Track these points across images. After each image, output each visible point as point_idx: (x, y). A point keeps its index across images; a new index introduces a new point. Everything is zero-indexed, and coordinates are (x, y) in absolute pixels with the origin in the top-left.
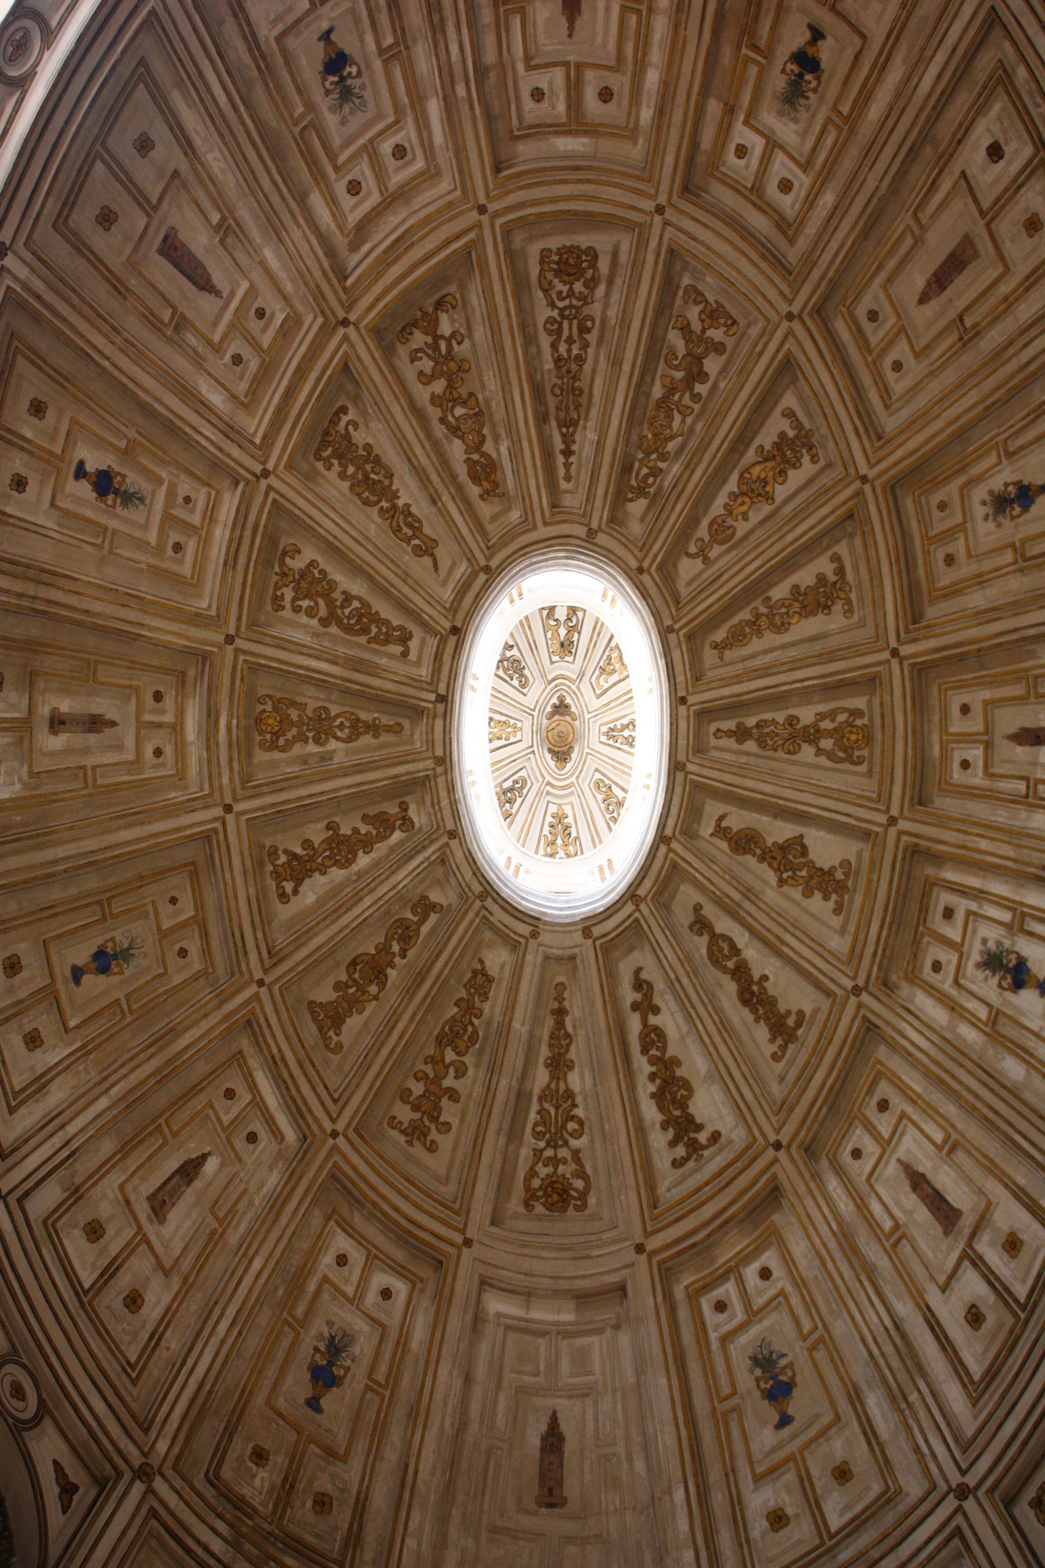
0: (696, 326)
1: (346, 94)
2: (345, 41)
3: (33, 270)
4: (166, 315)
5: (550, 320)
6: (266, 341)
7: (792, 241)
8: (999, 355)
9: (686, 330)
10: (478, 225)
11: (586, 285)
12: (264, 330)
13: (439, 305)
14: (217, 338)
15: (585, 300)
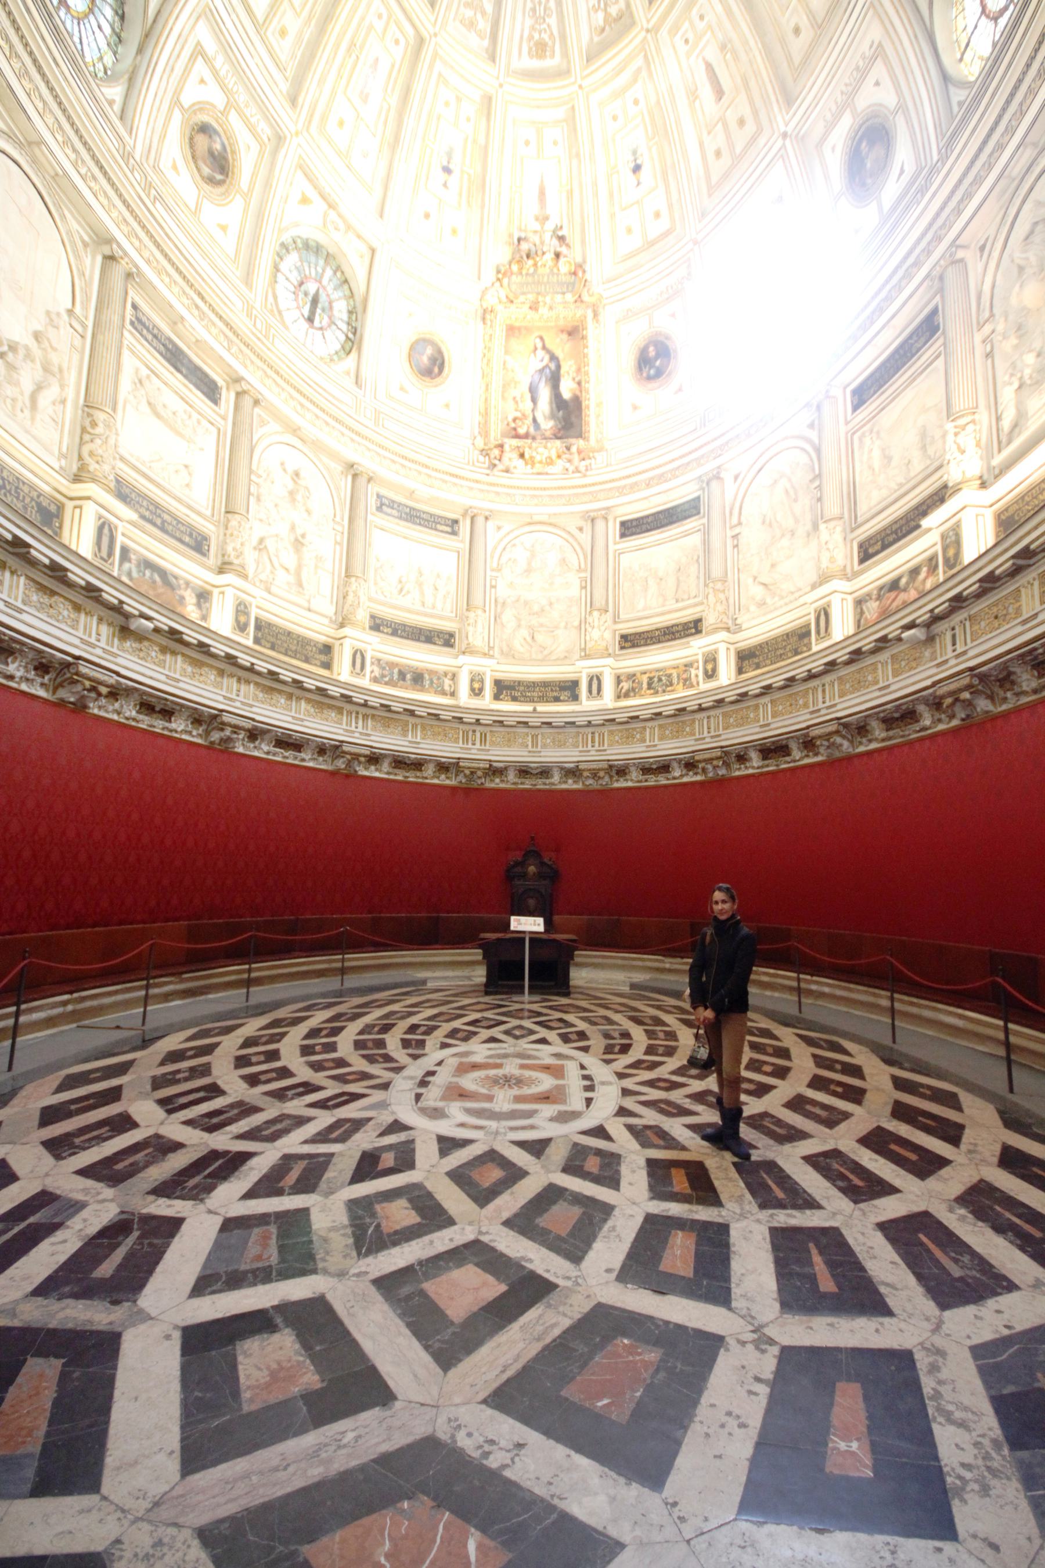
0: (479, 16)
1: (635, 153)
2: (632, 178)
3: (775, 118)
4: (728, 56)
5: (549, 16)
6: (686, 25)
7: (440, 75)
8: (337, 46)
9: (484, 13)
10: (583, 78)
11: (533, 37)
12: (686, 31)
13: (603, 30)
14: (709, 34)
15: (533, 28)
